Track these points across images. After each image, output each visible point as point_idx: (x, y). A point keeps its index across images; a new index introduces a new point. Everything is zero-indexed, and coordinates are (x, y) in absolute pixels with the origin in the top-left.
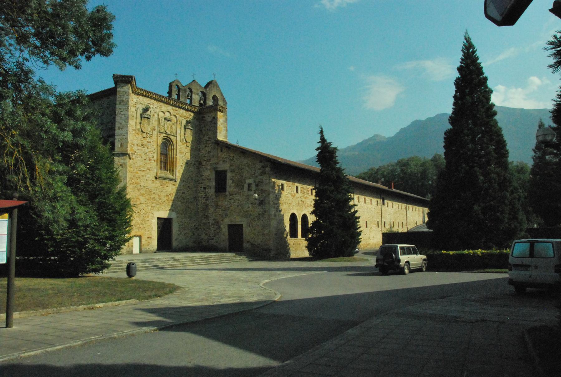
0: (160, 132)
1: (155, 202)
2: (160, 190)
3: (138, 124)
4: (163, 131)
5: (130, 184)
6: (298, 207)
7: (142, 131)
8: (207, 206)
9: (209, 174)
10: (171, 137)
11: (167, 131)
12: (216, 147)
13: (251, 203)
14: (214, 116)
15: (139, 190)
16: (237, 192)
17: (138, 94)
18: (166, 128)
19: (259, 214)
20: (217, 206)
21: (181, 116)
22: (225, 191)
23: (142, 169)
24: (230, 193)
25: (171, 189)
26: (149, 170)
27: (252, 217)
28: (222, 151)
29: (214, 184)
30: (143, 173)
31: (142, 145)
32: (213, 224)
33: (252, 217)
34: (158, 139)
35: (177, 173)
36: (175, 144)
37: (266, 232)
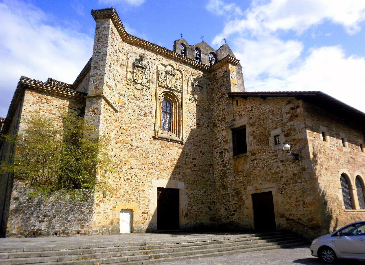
0: (160, 86)
1: (153, 167)
2: (161, 153)
3: (129, 73)
4: (164, 84)
5: (116, 142)
6: (350, 166)
7: (135, 81)
8: (224, 173)
9: (224, 135)
11: (170, 86)
12: (231, 102)
13: (282, 161)
14: (225, 69)
15: (129, 151)
16: (261, 150)
17: (131, 44)
18: (168, 83)
19: (295, 175)
20: (237, 172)
22: (245, 151)
23: (134, 125)
24: (251, 152)
25: (176, 151)
26: (145, 127)
27: (284, 180)
28: (237, 104)
29: (231, 145)
30: (136, 131)
32: (233, 196)
33: (284, 180)
34: (156, 93)
35: (184, 134)
37: (308, 200)
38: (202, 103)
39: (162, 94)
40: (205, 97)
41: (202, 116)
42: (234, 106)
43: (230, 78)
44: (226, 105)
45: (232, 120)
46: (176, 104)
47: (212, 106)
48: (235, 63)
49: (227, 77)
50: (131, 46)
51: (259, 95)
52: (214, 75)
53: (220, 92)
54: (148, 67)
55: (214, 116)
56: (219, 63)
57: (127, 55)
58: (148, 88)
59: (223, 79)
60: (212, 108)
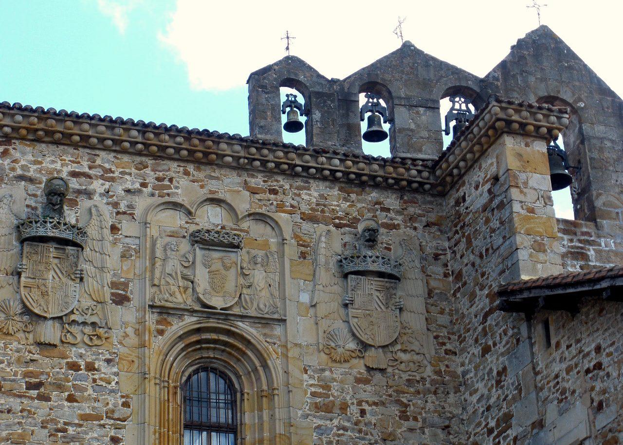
4: (180, 299)
10: (245, 328)
11: (218, 302)
14: (494, 169)
31: (37, 386)
36: (276, 363)
39: (181, 345)
40: (416, 321)
41: (407, 419)
42: (536, 348)
43: (511, 213)
44: (508, 352)
45: (534, 426)
46: (258, 379)
47: (458, 359)
48: (538, 128)
49: (501, 206)
51: (604, 284)
52: (457, 203)
53: (482, 288)
54: (92, 231)
55: (470, 410)
56: (464, 144)
58: (97, 332)
59: (487, 221)
60: (460, 370)
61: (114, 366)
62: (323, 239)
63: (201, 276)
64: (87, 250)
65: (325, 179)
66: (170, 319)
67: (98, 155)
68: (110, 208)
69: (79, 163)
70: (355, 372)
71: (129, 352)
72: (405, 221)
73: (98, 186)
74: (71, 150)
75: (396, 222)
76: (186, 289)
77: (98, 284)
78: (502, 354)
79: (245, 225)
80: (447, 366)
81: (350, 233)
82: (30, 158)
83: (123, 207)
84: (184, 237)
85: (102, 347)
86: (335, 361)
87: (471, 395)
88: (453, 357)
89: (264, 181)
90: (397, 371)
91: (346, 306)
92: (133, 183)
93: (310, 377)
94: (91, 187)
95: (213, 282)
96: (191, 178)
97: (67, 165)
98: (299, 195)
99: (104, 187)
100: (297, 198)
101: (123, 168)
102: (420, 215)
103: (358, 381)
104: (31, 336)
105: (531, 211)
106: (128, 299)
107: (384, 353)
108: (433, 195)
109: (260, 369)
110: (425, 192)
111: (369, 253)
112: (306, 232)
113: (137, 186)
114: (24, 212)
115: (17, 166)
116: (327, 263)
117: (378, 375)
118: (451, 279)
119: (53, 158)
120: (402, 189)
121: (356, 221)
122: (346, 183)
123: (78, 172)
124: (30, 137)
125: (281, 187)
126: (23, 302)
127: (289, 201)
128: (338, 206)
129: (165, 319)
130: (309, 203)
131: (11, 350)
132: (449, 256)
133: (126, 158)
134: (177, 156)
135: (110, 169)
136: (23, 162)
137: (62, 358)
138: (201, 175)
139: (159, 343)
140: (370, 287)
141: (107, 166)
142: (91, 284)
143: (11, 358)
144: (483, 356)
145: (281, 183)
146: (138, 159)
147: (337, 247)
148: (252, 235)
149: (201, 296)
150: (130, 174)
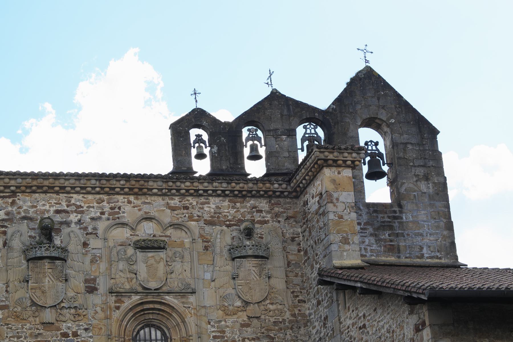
10: (170, 299)
11: (153, 285)
21: (208, 223)
36: (191, 320)
38: (271, 307)
39: (131, 314)
40: (279, 283)
46: (180, 330)
47: (307, 306)
50: (13, 203)
57: (5, 233)
58: (78, 311)
60: (307, 312)
61: (89, 332)
62: (219, 236)
63: (142, 269)
64: (69, 261)
65: (219, 196)
66: (123, 299)
67: (72, 197)
68: (82, 231)
69: (60, 204)
70: (240, 320)
71: (99, 323)
72: (272, 218)
73: (74, 218)
74: (54, 196)
75: (266, 219)
76: (132, 279)
77: (78, 283)
78: (326, 308)
79: (168, 233)
80: (299, 310)
81: (236, 229)
82: (29, 204)
83: (90, 230)
84: (130, 245)
85: (82, 321)
86: (227, 314)
87: (313, 329)
88: (303, 304)
89: (180, 202)
90: (267, 317)
91: (234, 278)
92: (96, 213)
93: (213, 326)
94: (69, 219)
95: (149, 270)
96: (132, 205)
97: (53, 206)
98: (203, 208)
99: (77, 218)
100: (201, 211)
101: (89, 204)
102: (282, 212)
103: (242, 325)
104: (37, 319)
105: (341, 217)
106: (96, 289)
107: (259, 306)
108: (291, 198)
109: (181, 325)
110: (285, 197)
111: (248, 243)
112: (207, 233)
113: (98, 214)
114: (28, 241)
115: (21, 210)
116: (221, 251)
117: (255, 321)
118: (302, 253)
119: (43, 202)
120: (270, 197)
121: (240, 221)
122: (233, 196)
123: (61, 210)
124: (28, 191)
125: (191, 204)
126: (31, 299)
127: (196, 213)
128: (228, 212)
129: (120, 299)
130: (210, 212)
131: (26, 329)
132: (301, 238)
133: (90, 197)
134: (122, 192)
135: (81, 205)
136: (25, 208)
137: (58, 331)
138: (139, 202)
139: (117, 315)
140: (249, 265)
141: (78, 203)
142: (73, 282)
143: (26, 334)
144: (318, 306)
145: (191, 201)
146: (98, 196)
147: (228, 240)
148: (173, 239)
149: (141, 283)
150: (93, 207)
